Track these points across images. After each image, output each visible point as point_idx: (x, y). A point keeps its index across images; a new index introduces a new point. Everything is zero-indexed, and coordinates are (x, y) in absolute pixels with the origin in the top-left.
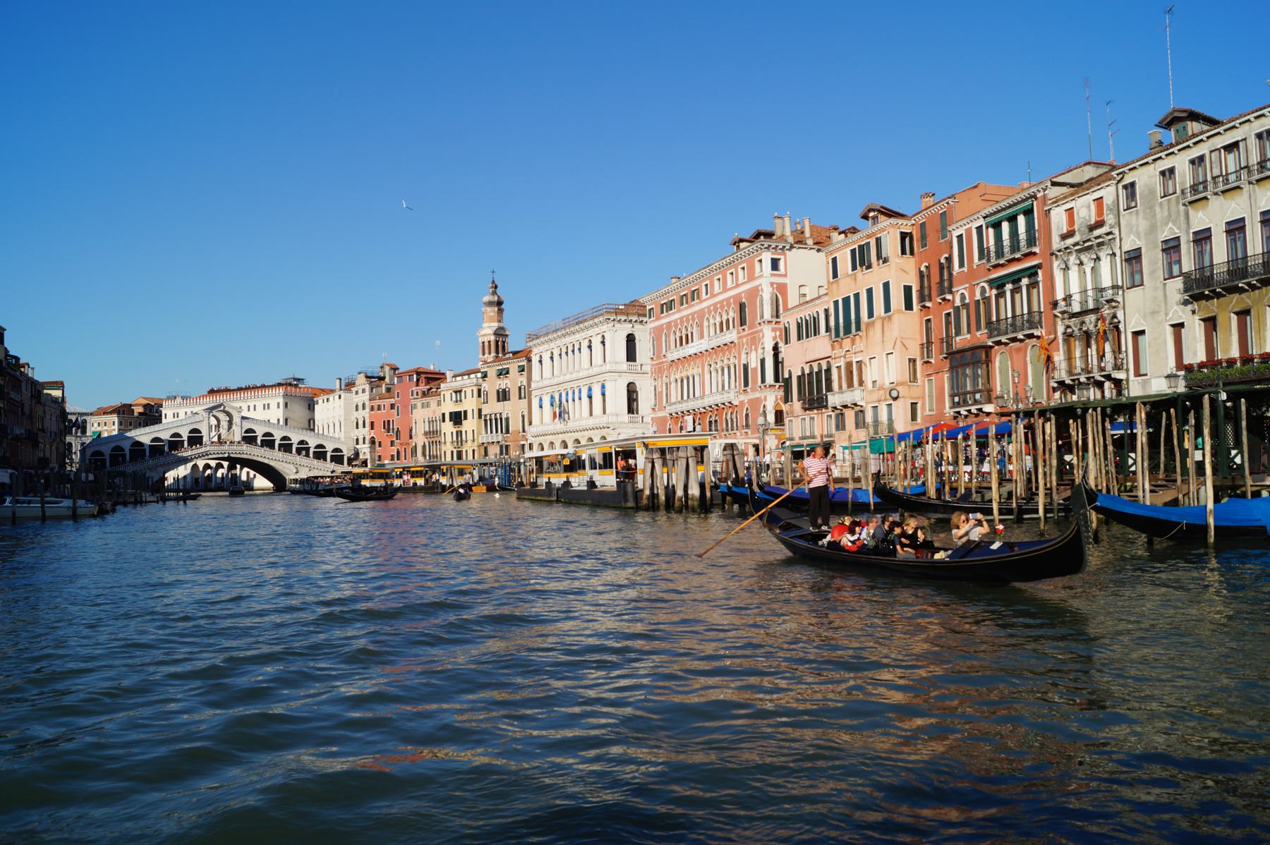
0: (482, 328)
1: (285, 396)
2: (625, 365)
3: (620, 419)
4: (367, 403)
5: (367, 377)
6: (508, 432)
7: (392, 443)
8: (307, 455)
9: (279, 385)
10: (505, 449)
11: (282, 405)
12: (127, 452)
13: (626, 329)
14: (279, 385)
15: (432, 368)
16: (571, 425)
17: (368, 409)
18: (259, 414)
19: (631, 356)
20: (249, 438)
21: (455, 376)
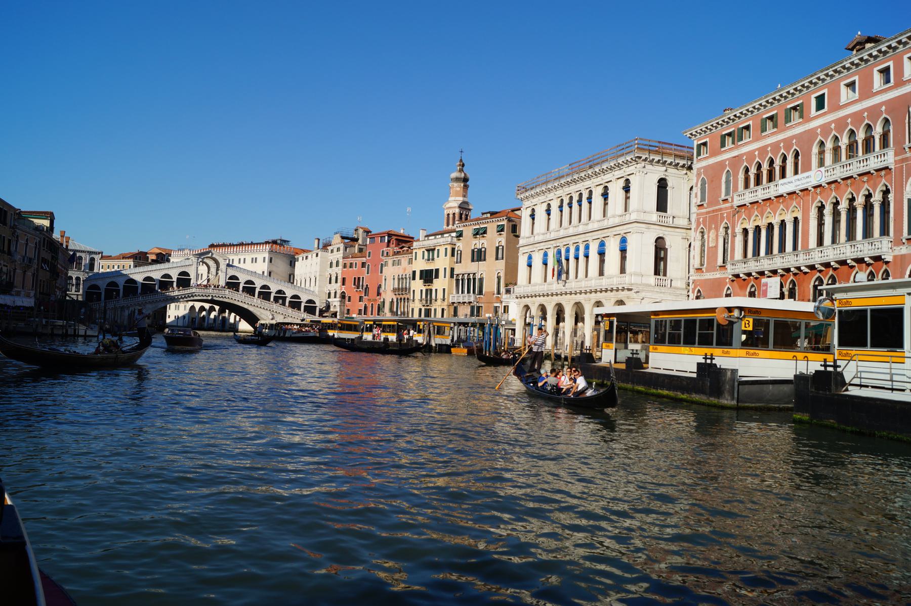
0: (447, 201)
1: (271, 251)
2: (654, 216)
3: (645, 281)
4: (341, 261)
5: (343, 238)
6: (481, 292)
7: (361, 299)
9: (267, 243)
10: (476, 310)
11: (267, 260)
12: (121, 288)
13: (658, 172)
14: (267, 243)
15: (402, 231)
16: (572, 284)
17: (341, 267)
18: (249, 266)
19: (662, 206)
20: (232, 284)
21: (427, 236)
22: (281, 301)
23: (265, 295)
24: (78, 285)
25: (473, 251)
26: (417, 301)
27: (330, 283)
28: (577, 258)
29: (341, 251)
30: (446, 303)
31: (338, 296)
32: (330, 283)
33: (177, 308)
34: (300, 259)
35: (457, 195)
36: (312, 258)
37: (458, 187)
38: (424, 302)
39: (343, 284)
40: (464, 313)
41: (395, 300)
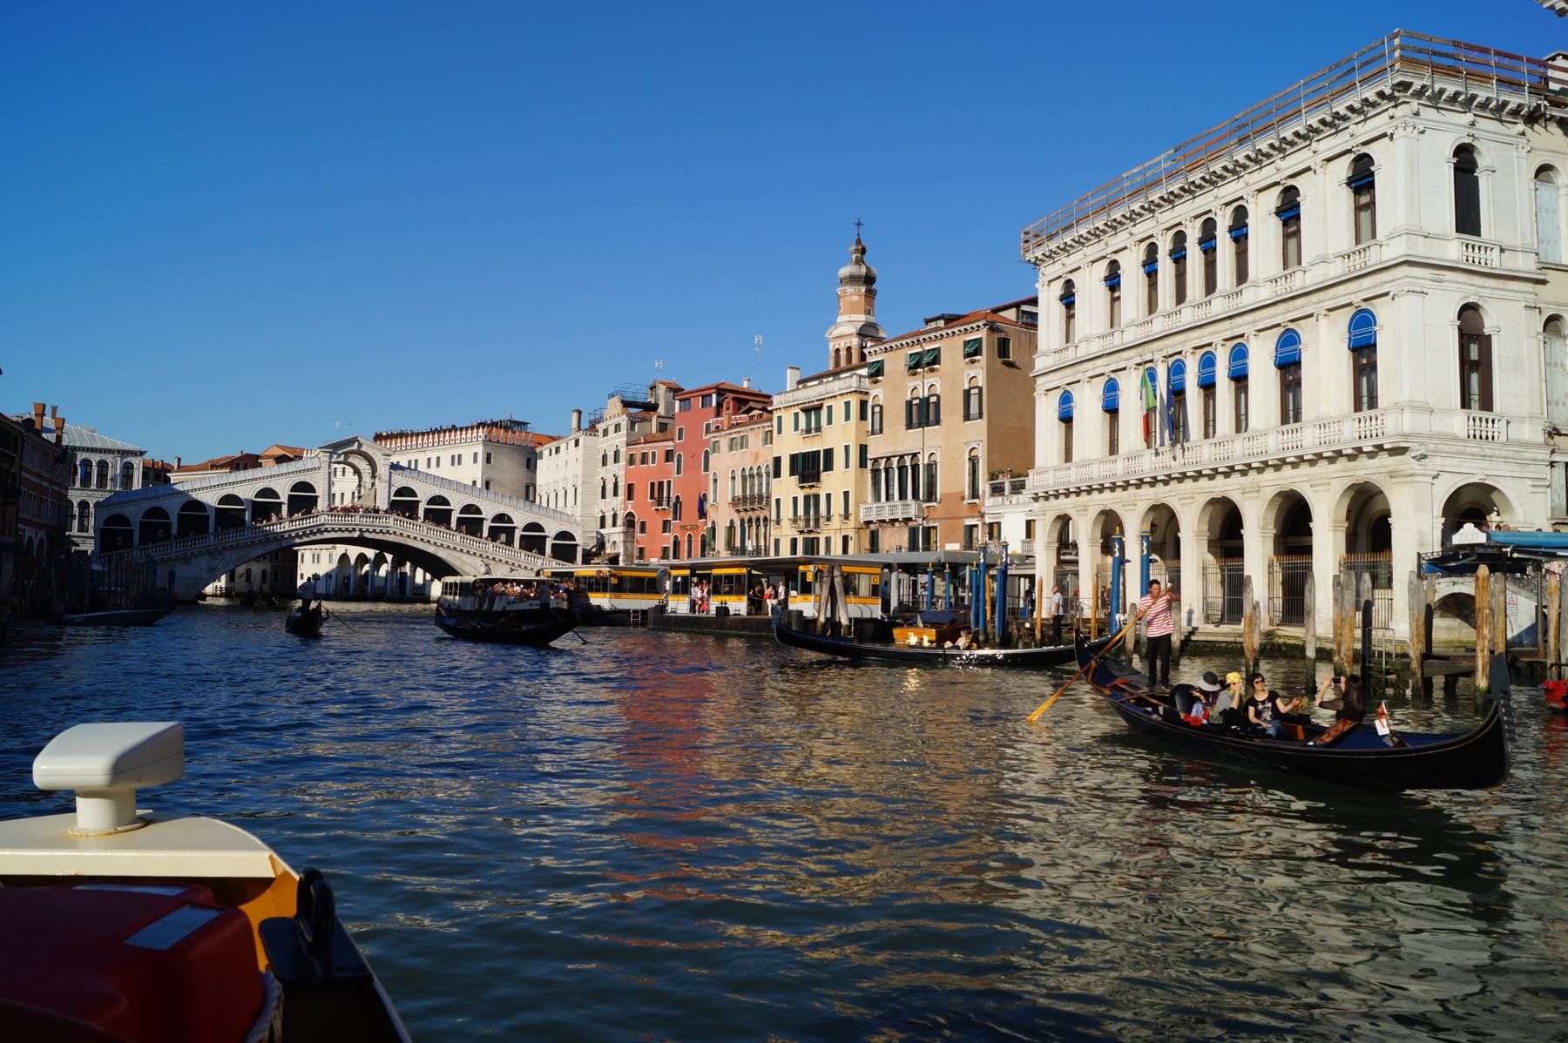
1: (488, 441)
2: (1453, 249)
3: (1438, 425)
4: (623, 450)
5: (626, 404)
6: (931, 495)
7: (666, 526)
8: (510, 542)
9: (483, 425)
10: (921, 537)
12: (174, 519)
13: (1452, 128)
14: (483, 425)
15: (745, 385)
16: (1200, 452)
17: (623, 462)
18: (446, 471)
19: (1467, 219)
20: (404, 505)
22: (503, 537)
23: (471, 524)
24: (83, 516)
25: (909, 404)
26: (785, 523)
27: (604, 496)
28: (1208, 387)
29: (624, 431)
30: (851, 523)
31: (620, 521)
32: (604, 496)
33: (316, 559)
34: (546, 453)
35: (853, 311)
36: (567, 447)
37: (854, 294)
38: (802, 524)
39: (630, 498)
40: (894, 543)
41: (737, 524)
